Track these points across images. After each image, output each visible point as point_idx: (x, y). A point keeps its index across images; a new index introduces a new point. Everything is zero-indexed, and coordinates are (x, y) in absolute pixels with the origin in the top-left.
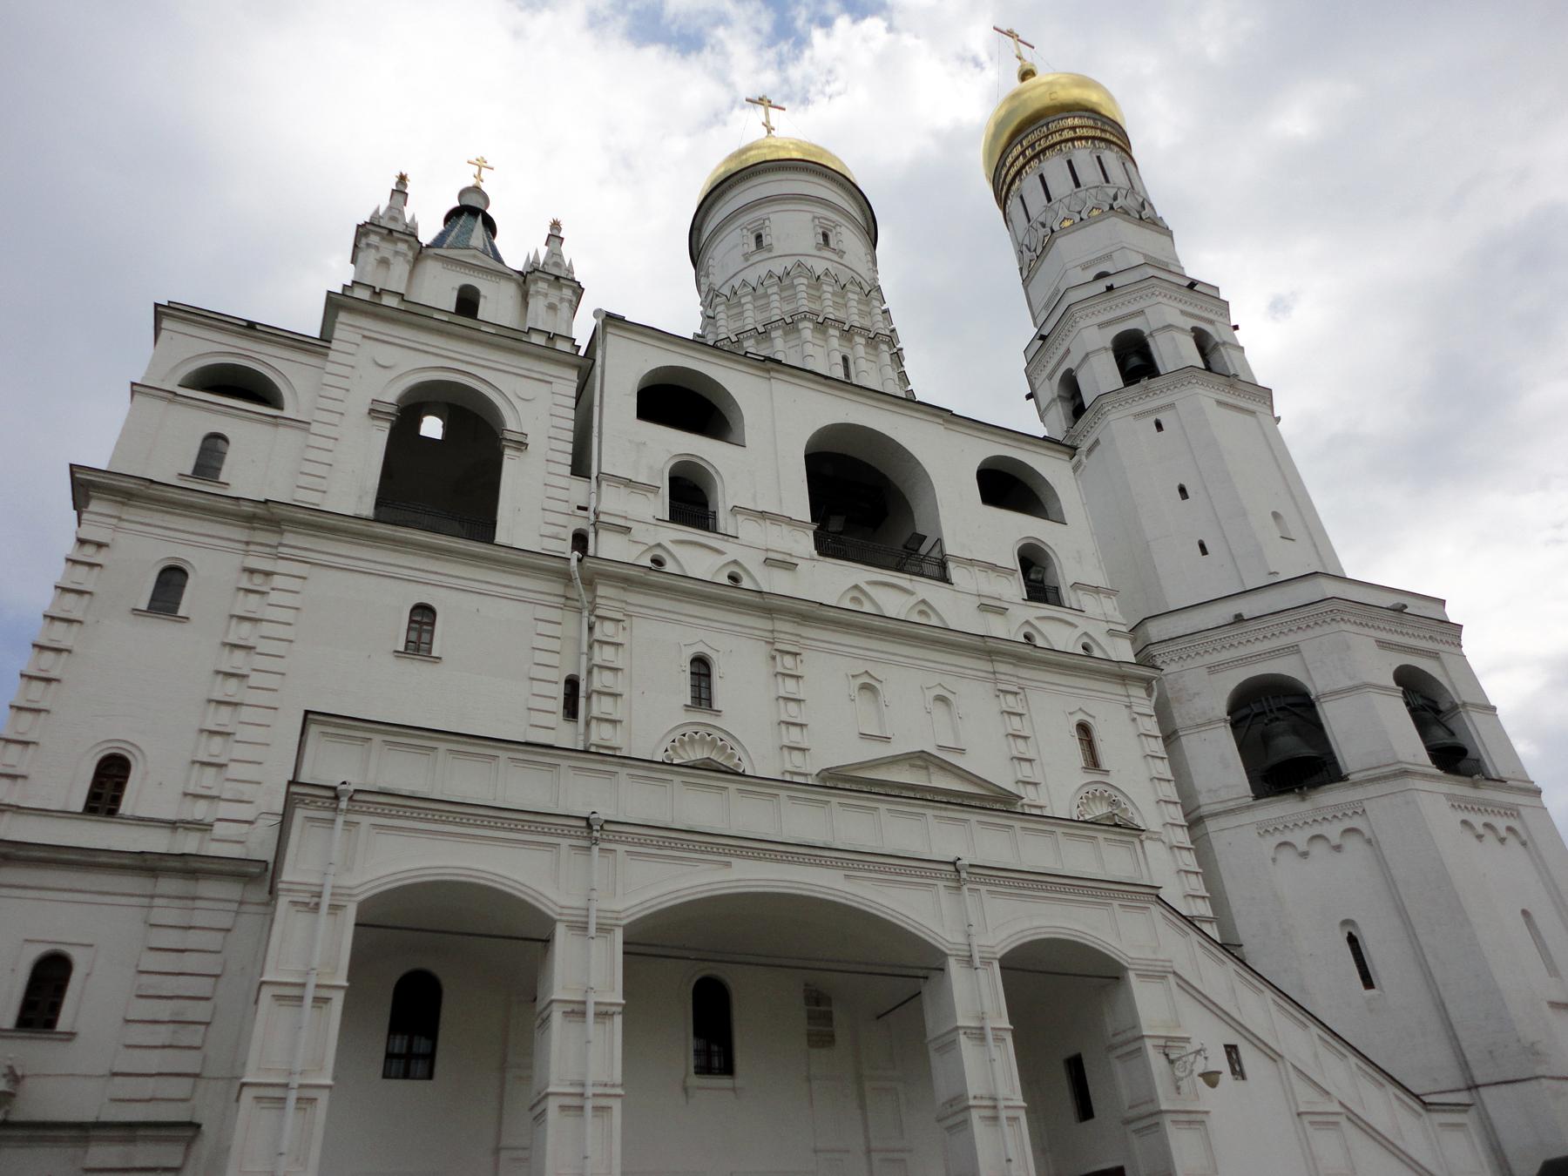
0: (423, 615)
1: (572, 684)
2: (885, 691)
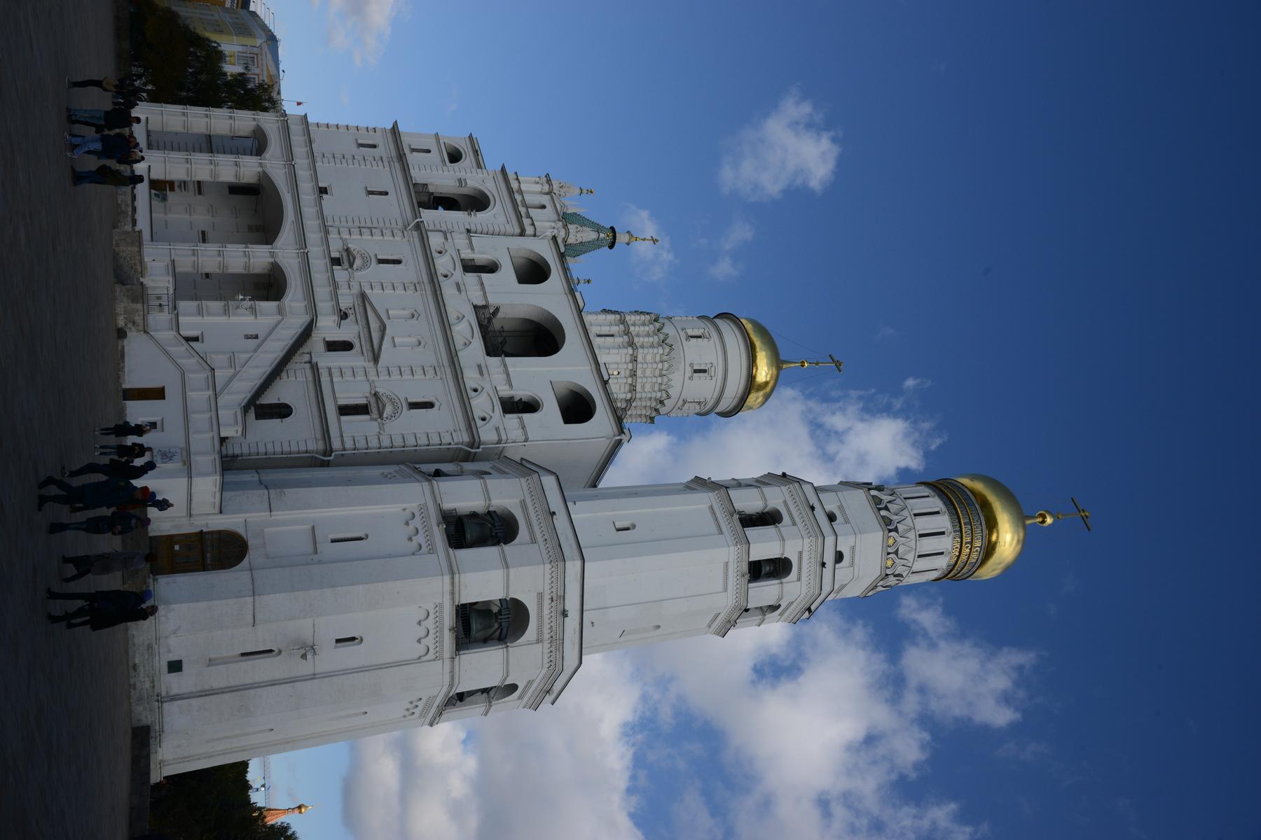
0: (386, 193)
2: (414, 321)
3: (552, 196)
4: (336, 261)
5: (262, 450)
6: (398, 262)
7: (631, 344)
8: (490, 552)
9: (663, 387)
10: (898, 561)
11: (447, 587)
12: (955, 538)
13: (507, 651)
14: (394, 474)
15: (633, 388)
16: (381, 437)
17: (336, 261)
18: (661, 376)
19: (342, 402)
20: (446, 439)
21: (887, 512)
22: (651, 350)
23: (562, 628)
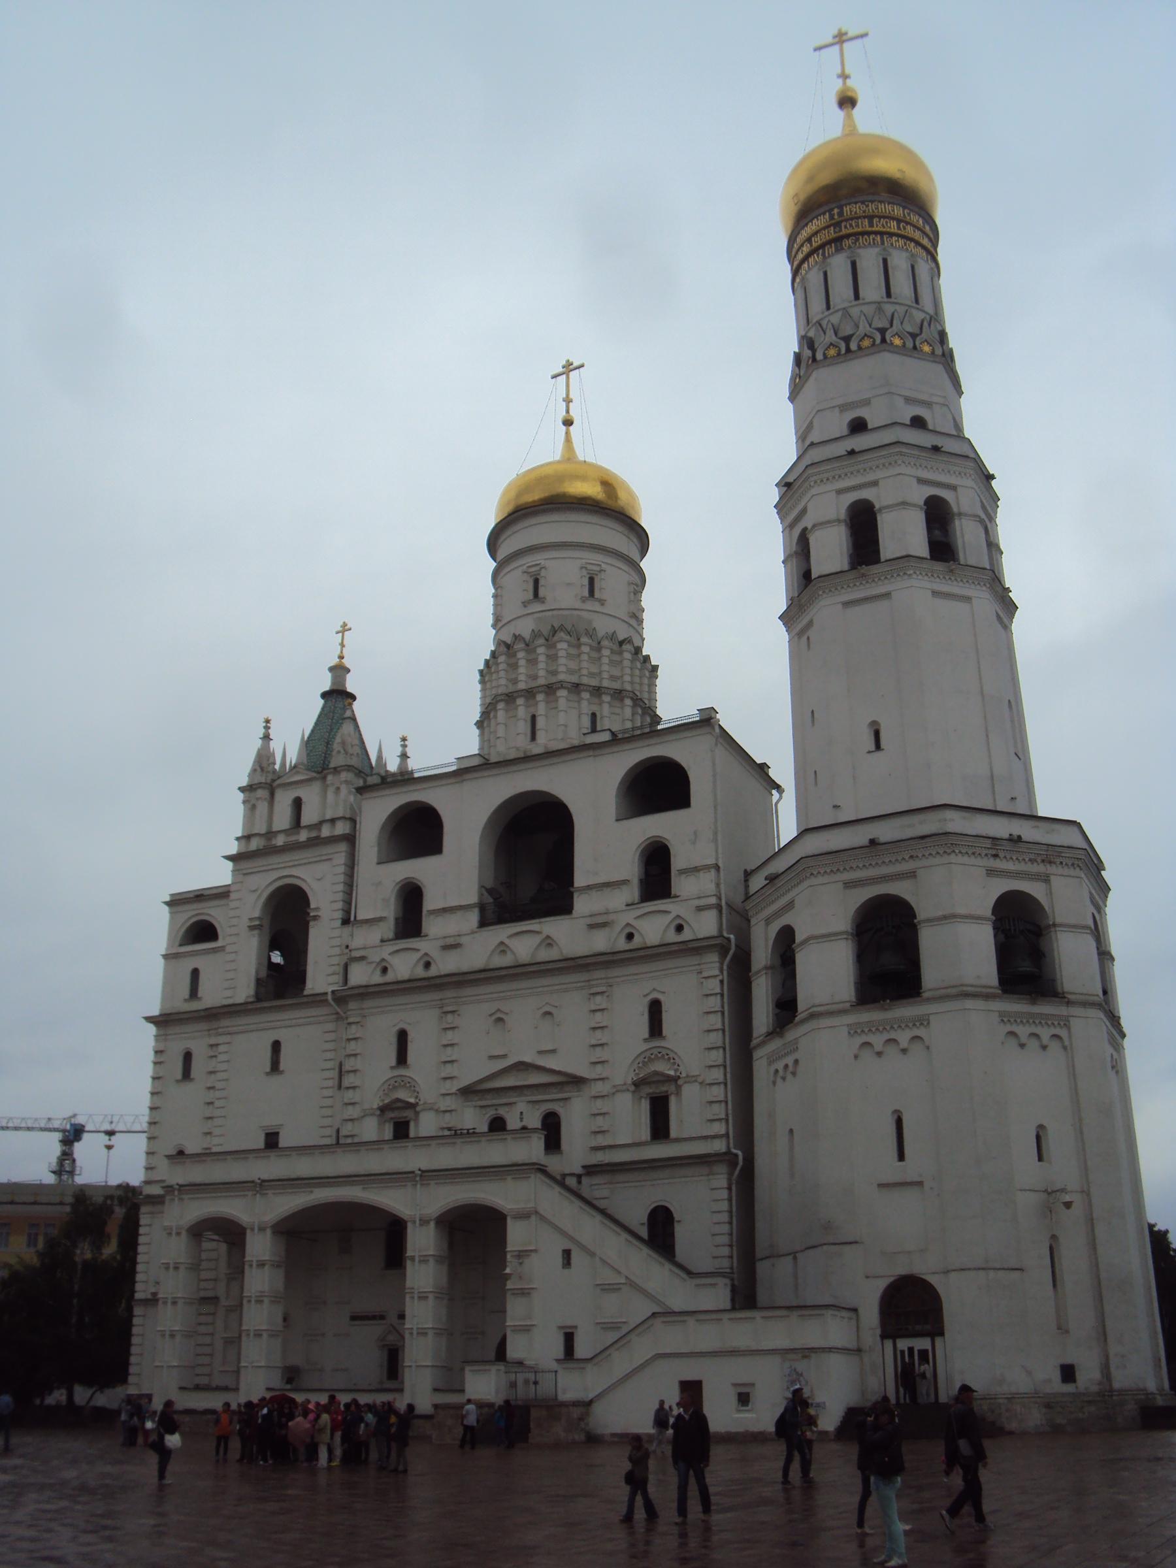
0: (276, 1046)
1: (341, 1065)
3: (280, 786)
4: (401, 1131)
5: (726, 1251)
6: (402, 1037)
7: (550, 690)
8: (929, 940)
9: (616, 647)
10: (924, 336)
11: (980, 1004)
12: (892, 244)
13: (1061, 925)
14: (780, 1065)
15: (618, 695)
16: (708, 1082)
17: (401, 1131)
18: (598, 648)
19: (645, 1134)
20: (714, 986)
21: (854, 337)
22: (562, 661)
23: (1030, 846)
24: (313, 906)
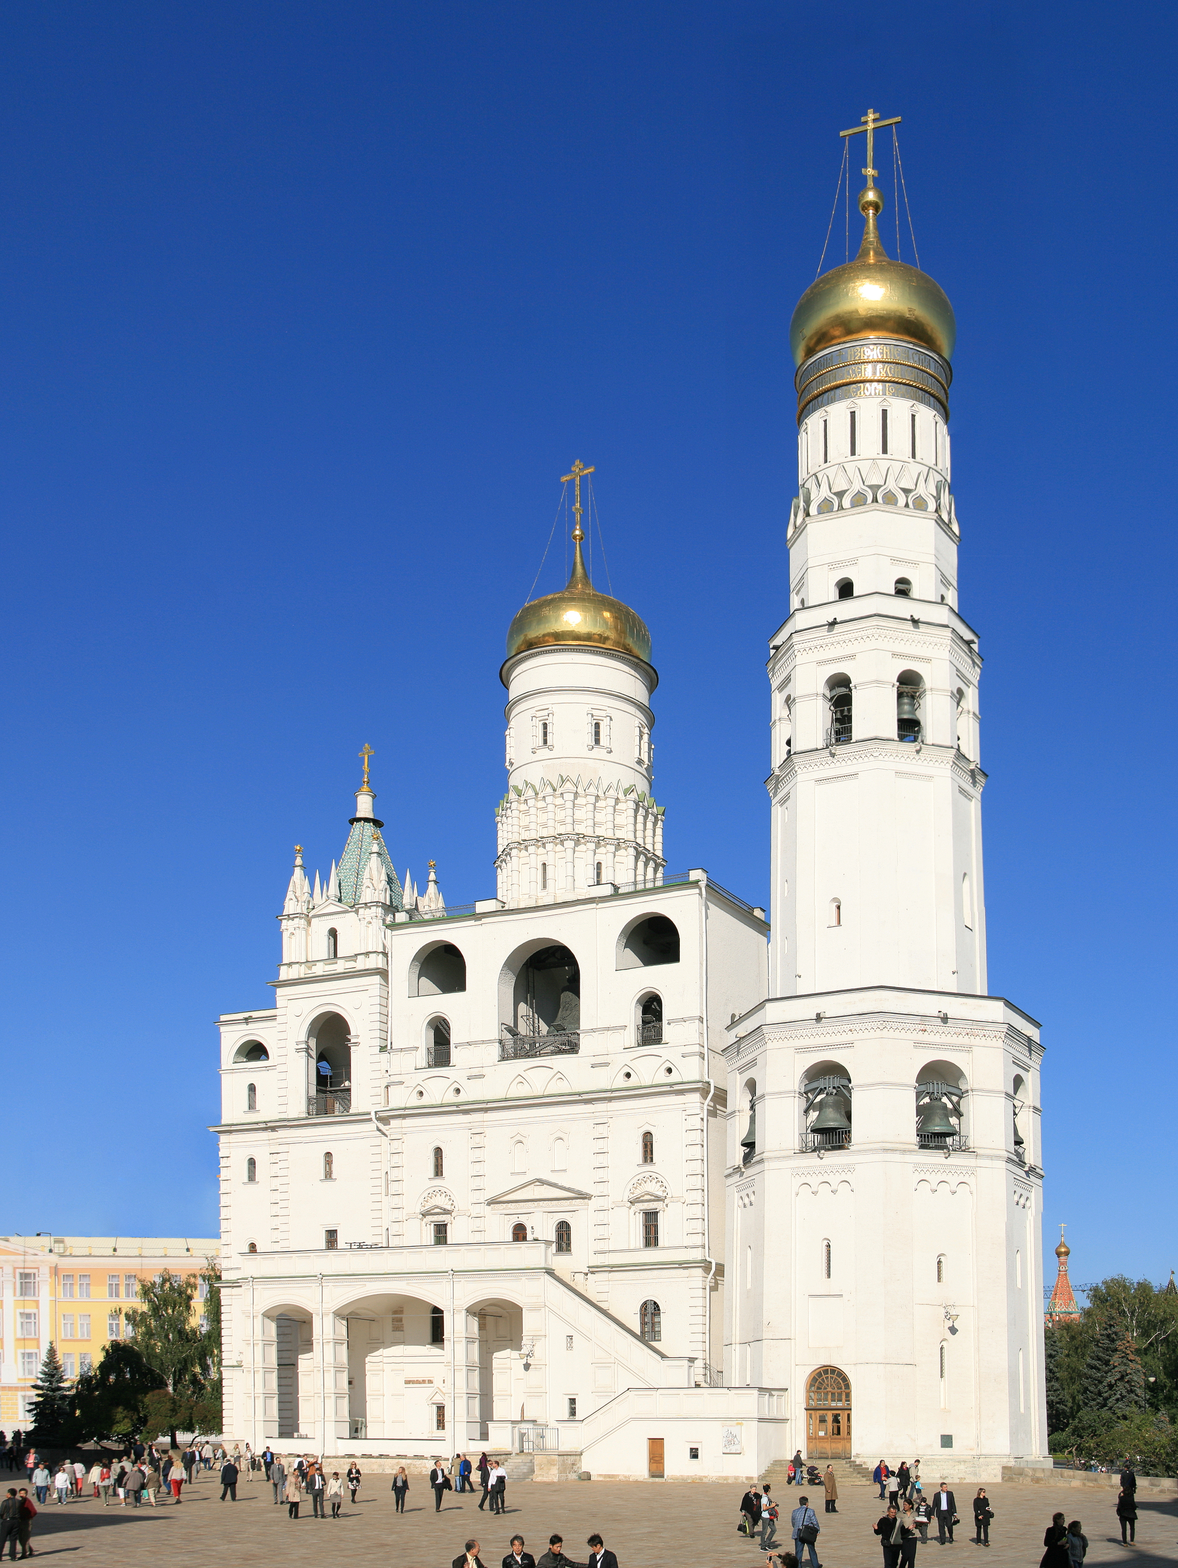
24: (353, 1032)
